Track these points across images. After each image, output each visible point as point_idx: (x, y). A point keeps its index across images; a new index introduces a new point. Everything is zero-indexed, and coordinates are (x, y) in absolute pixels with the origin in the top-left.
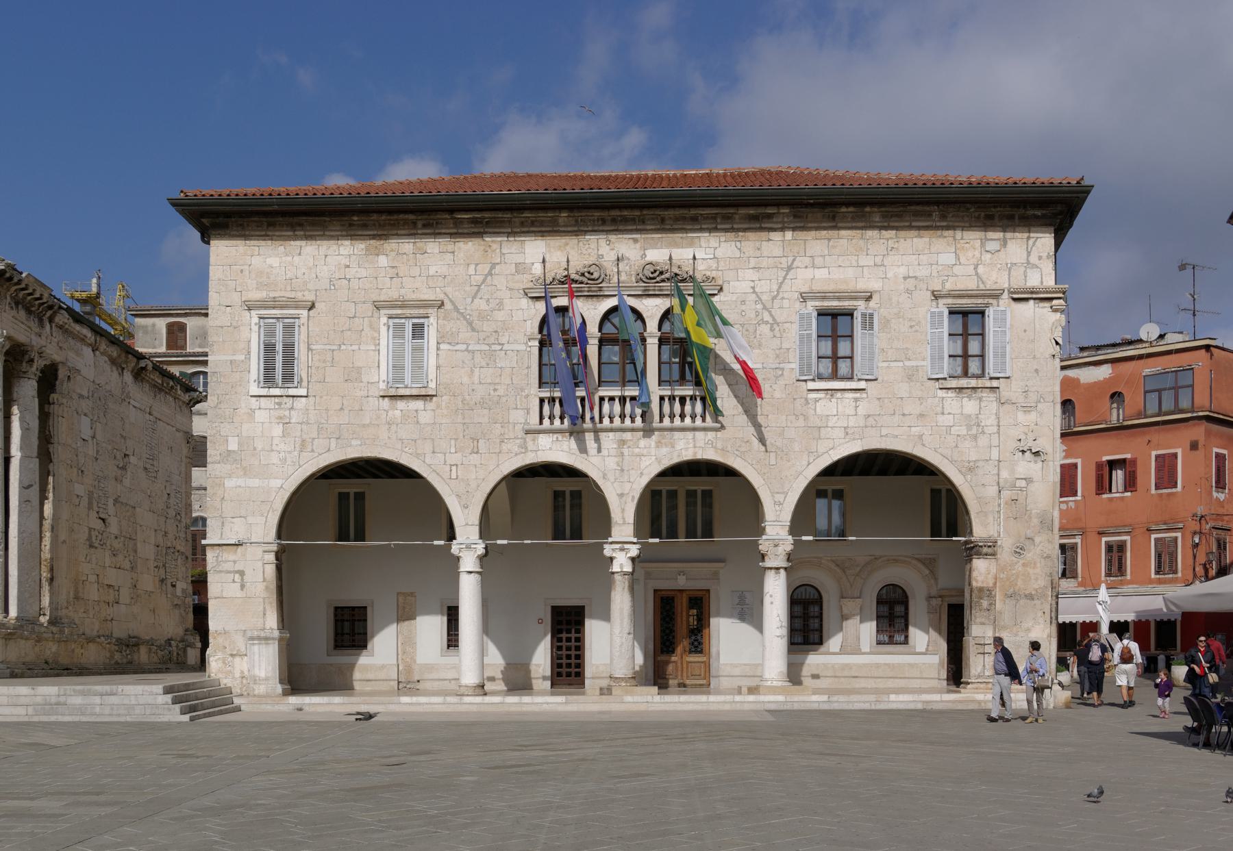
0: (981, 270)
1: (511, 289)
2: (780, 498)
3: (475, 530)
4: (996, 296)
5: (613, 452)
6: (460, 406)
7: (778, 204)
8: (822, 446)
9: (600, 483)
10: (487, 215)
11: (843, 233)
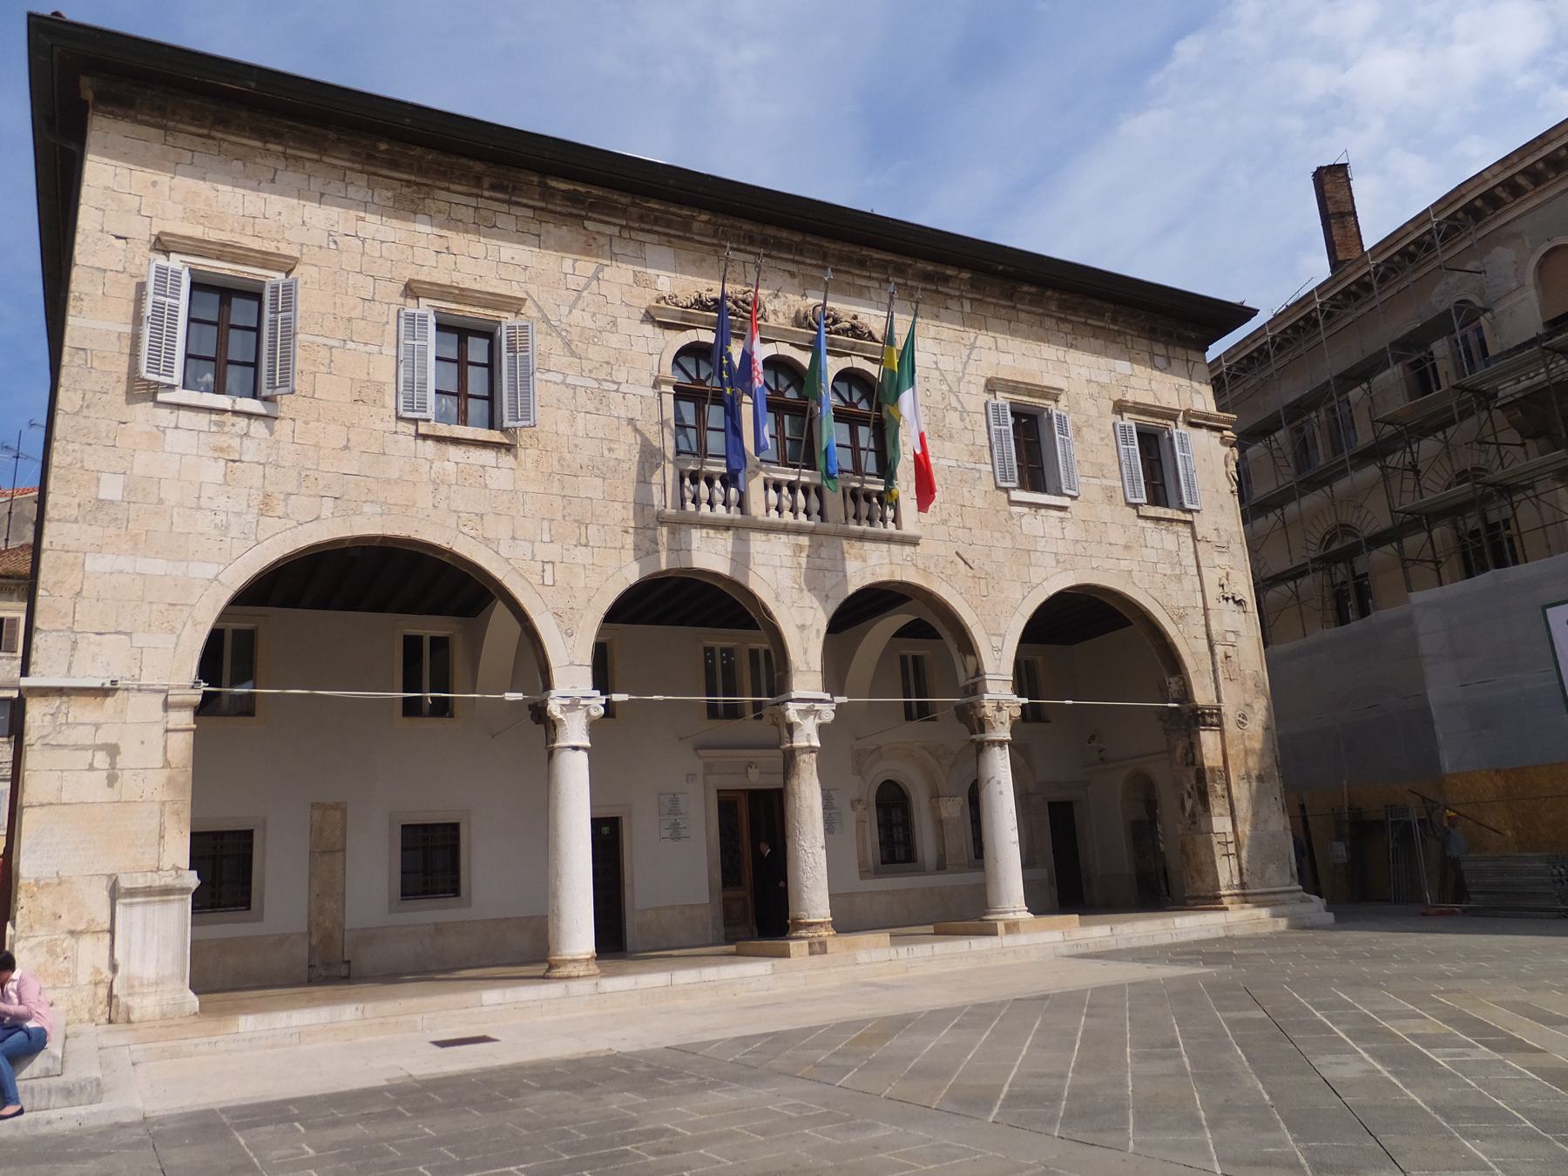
0: (1154, 385)
1: (628, 305)
2: (996, 641)
3: (587, 673)
4: (1171, 415)
5: (788, 562)
6: (556, 467)
7: (961, 265)
8: (1035, 576)
9: (772, 606)
11: (1022, 316)
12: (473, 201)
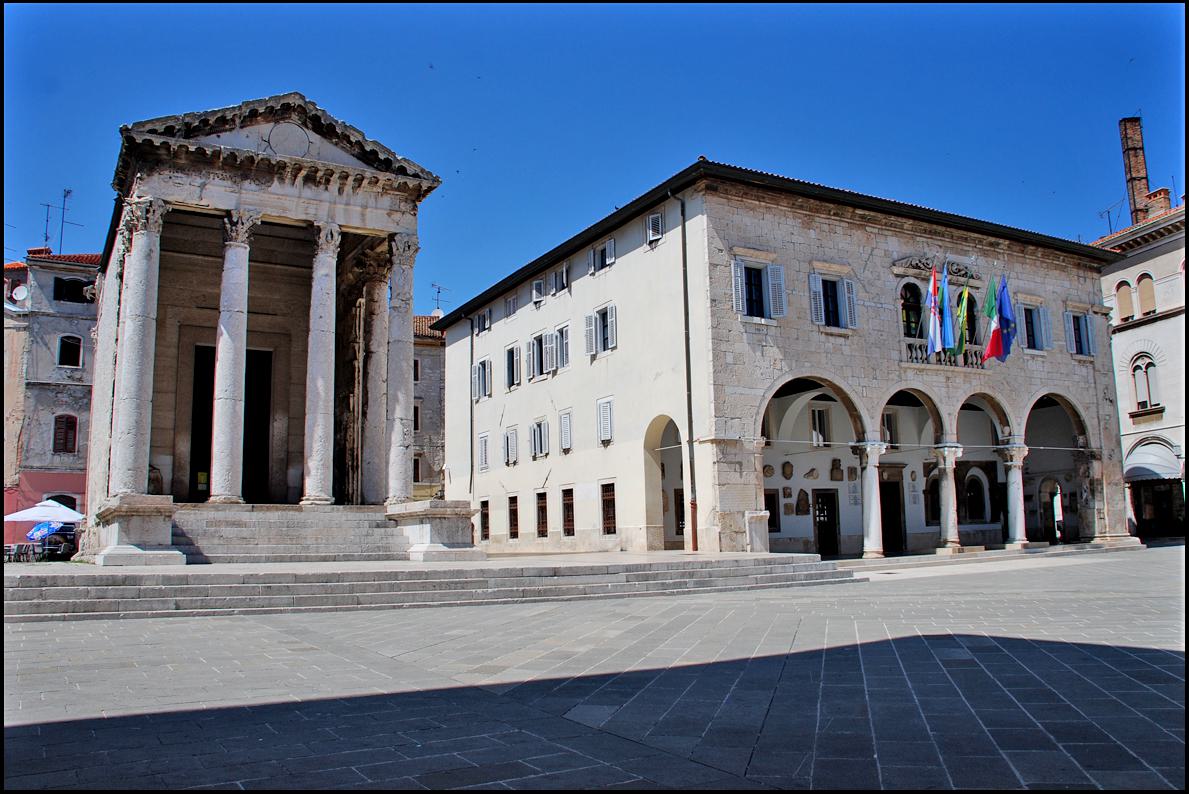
10: (872, 214)
12: (827, 221)
